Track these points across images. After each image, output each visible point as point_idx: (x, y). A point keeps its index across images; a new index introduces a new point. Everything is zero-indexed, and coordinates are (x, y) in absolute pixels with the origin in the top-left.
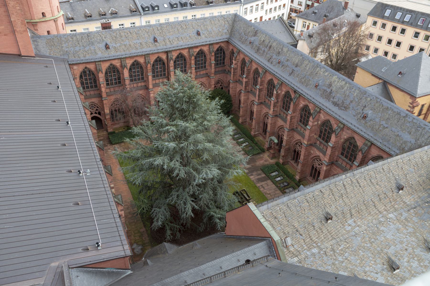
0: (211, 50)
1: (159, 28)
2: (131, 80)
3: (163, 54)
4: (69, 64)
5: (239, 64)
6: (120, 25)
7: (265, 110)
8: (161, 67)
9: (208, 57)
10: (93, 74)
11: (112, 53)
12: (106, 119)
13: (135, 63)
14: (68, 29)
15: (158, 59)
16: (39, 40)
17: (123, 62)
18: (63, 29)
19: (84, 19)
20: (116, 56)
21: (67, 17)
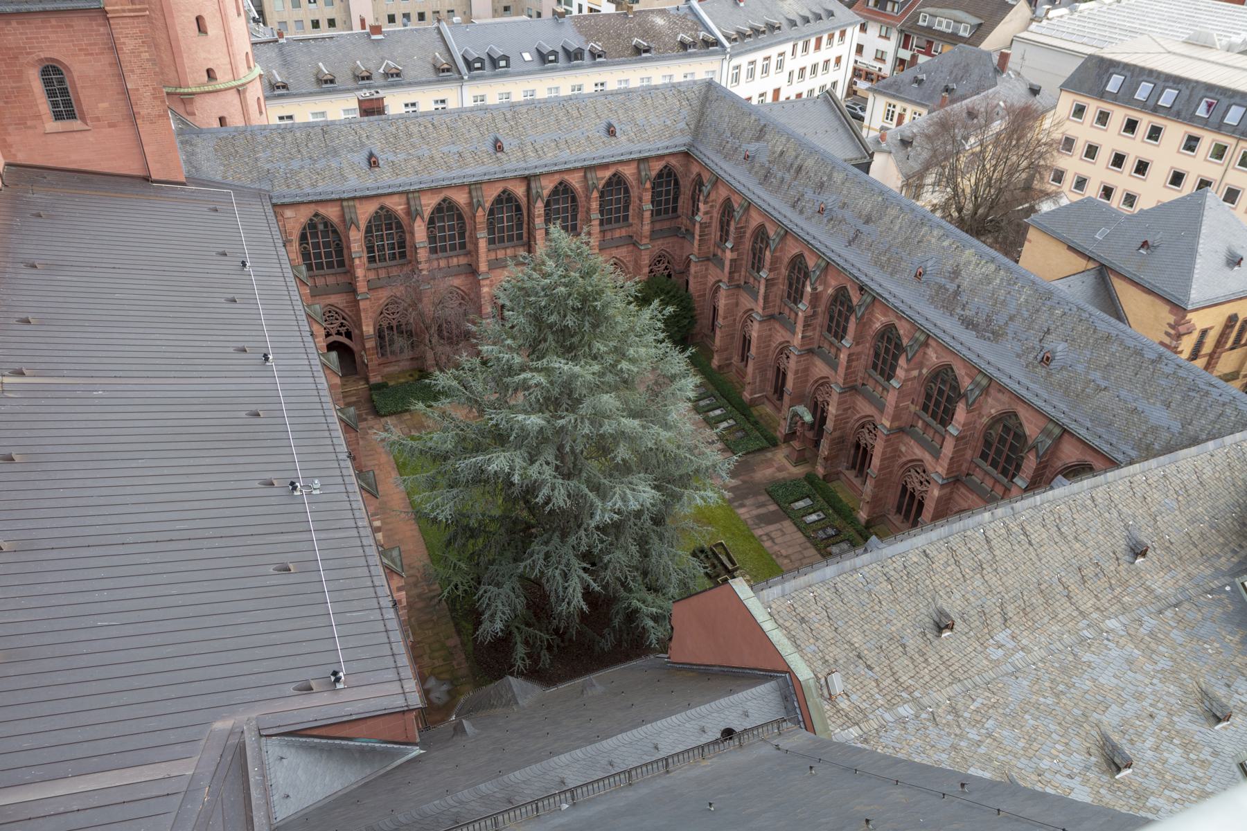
0: (643, 174)
1: (509, 116)
2: (433, 250)
3: (518, 183)
4: (274, 205)
5: (716, 214)
6: (406, 105)
7: (780, 335)
8: (511, 216)
9: (634, 193)
10: (335, 232)
11: (385, 179)
12: (364, 349)
13: (445, 205)
14: (273, 113)
15: (504, 197)
16: (196, 140)
17: (412, 203)
18: (261, 113)
19: (315, 88)
20: (394, 186)
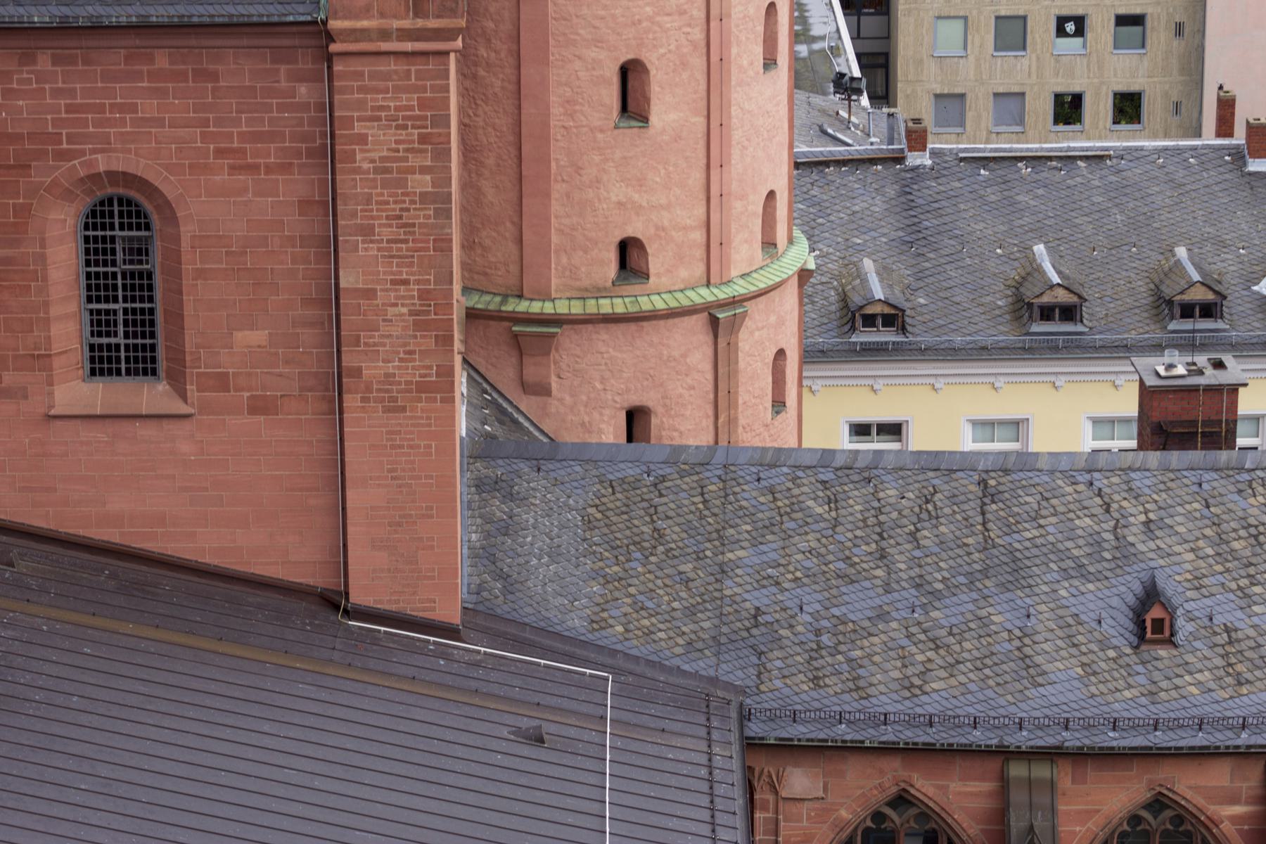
4: (751, 745)
16: (532, 483)
18: (779, 404)
19: (1005, 334)
20: (1221, 723)
21: (844, 299)
